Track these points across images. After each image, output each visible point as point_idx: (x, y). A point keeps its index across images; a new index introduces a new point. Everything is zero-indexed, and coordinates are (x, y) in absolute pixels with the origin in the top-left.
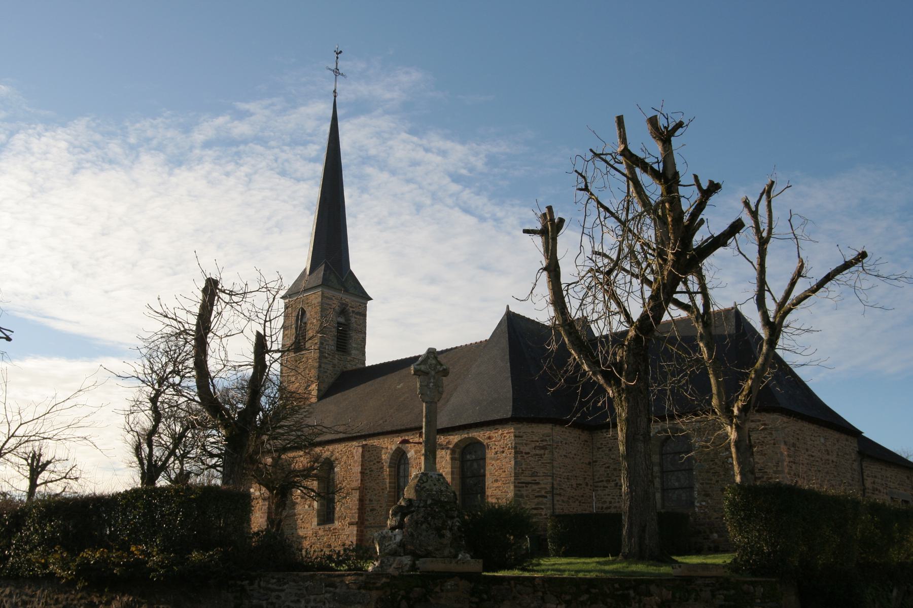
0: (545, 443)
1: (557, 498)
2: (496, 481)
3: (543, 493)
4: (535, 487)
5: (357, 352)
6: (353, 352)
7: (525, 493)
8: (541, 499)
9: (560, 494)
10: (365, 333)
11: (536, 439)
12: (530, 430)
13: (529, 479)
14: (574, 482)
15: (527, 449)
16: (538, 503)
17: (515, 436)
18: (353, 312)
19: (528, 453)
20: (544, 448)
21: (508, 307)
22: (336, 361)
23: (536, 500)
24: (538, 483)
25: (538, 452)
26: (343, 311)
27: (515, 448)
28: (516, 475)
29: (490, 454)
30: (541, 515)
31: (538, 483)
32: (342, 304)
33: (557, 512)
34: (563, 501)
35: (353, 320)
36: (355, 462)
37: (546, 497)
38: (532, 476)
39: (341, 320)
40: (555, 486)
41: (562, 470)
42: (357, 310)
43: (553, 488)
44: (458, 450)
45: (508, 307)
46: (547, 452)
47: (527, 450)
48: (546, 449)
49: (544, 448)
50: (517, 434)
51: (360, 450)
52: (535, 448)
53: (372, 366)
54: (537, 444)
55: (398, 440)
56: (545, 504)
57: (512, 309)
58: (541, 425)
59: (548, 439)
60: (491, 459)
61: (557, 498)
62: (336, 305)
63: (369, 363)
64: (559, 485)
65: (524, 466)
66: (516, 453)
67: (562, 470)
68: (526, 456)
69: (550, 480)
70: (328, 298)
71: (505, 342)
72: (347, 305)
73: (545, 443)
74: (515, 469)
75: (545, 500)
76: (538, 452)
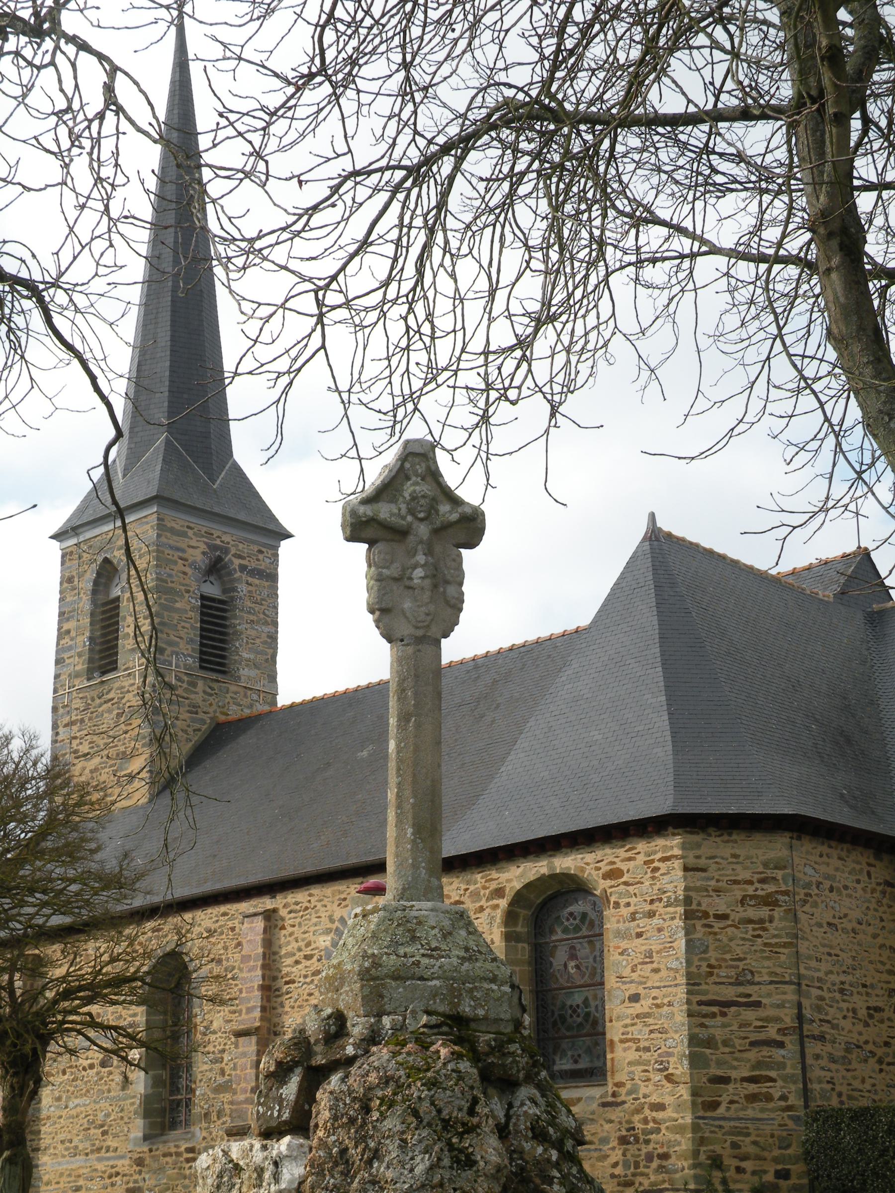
0: (771, 888)
1: (813, 1048)
2: (635, 998)
3: (772, 1032)
4: (749, 1015)
5: (253, 673)
6: (245, 672)
7: (719, 1034)
8: (765, 1051)
9: (821, 1038)
10: (275, 624)
11: (745, 875)
12: (726, 851)
13: (729, 993)
14: (860, 1003)
15: (720, 905)
16: (759, 1065)
17: (686, 869)
18: (243, 568)
19: (725, 917)
20: (769, 901)
21: (652, 517)
22: (198, 698)
23: (753, 1055)
24: (757, 1004)
25: (752, 913)
26: (216, 568)
27: (688, 901)
28: (693, 981)
29: (613, 921)
30: (769, 1098)
31: (757, 1004)
32: (214, 548)
33: (817, 1102)
34: (833, 1060)
35: (242, 588)
36: (246, 959)
37: (781, 1045)
38: (738, 983)
39: (213, 590)
40: (807, 1013)
41: (824, 967)
42: (252, 564)
43: (800, 1017)
44: (523, 913)
45: (652, 517)
46: (778, 913)
47: (722, 909)
48: (776, 903)
49: (769, 901)
50: (691, 861)
51: (259, 924)
52: (742, 902)
53: (292, 706)
54: (750, 890)
55: (256, 548)
56: (781, 1066)
57: (664, 524)
58: (758, 836)
59: (779, 874)
60: (618, 934)
61: (813, 1048)
62: (198, 555)
63: (283, 700)
64: (819, 1009)
65: (713, 955)
66: (688, 916)
67: (824, 967)
68: (717, 925)
69: (790, 994)
70: (172, 531)
71: (647, 617)
72: (227, 551)
73: (771, 888)
74: (689, 962)
75: (778, 1054)
76: (752, 913)
